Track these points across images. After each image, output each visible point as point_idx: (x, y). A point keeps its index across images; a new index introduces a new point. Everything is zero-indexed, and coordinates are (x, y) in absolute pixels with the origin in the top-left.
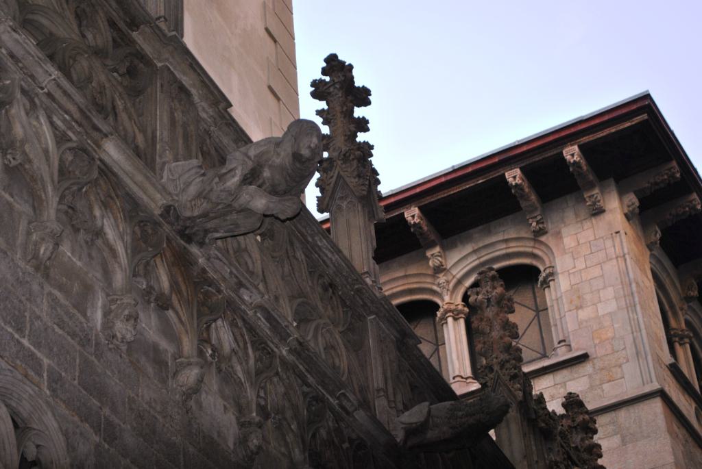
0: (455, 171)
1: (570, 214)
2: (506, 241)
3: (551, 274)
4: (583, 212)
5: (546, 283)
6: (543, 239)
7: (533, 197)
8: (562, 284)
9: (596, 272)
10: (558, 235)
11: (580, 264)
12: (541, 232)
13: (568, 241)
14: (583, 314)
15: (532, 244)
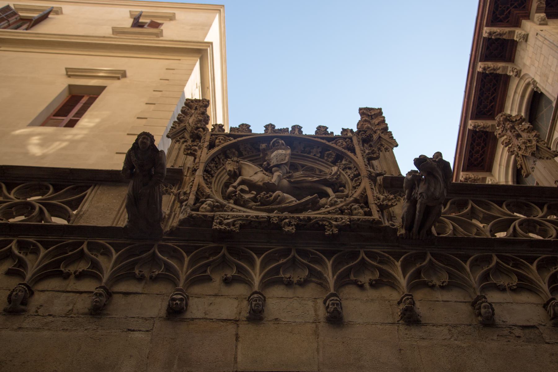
0: (465, 92)
1: (522, 53)
2: (515, 92)
3: (535, 81)
4: (523, 45)
5: (537, 88)
6: (522, 74)
7: (500, 65)
8: (537, 79)
9: (542, 57)
10: (525, 65)
11: (536, 64)
12: (518, 74)
13: (528, 62)
14: (550, 81)
15: (522, 82)
